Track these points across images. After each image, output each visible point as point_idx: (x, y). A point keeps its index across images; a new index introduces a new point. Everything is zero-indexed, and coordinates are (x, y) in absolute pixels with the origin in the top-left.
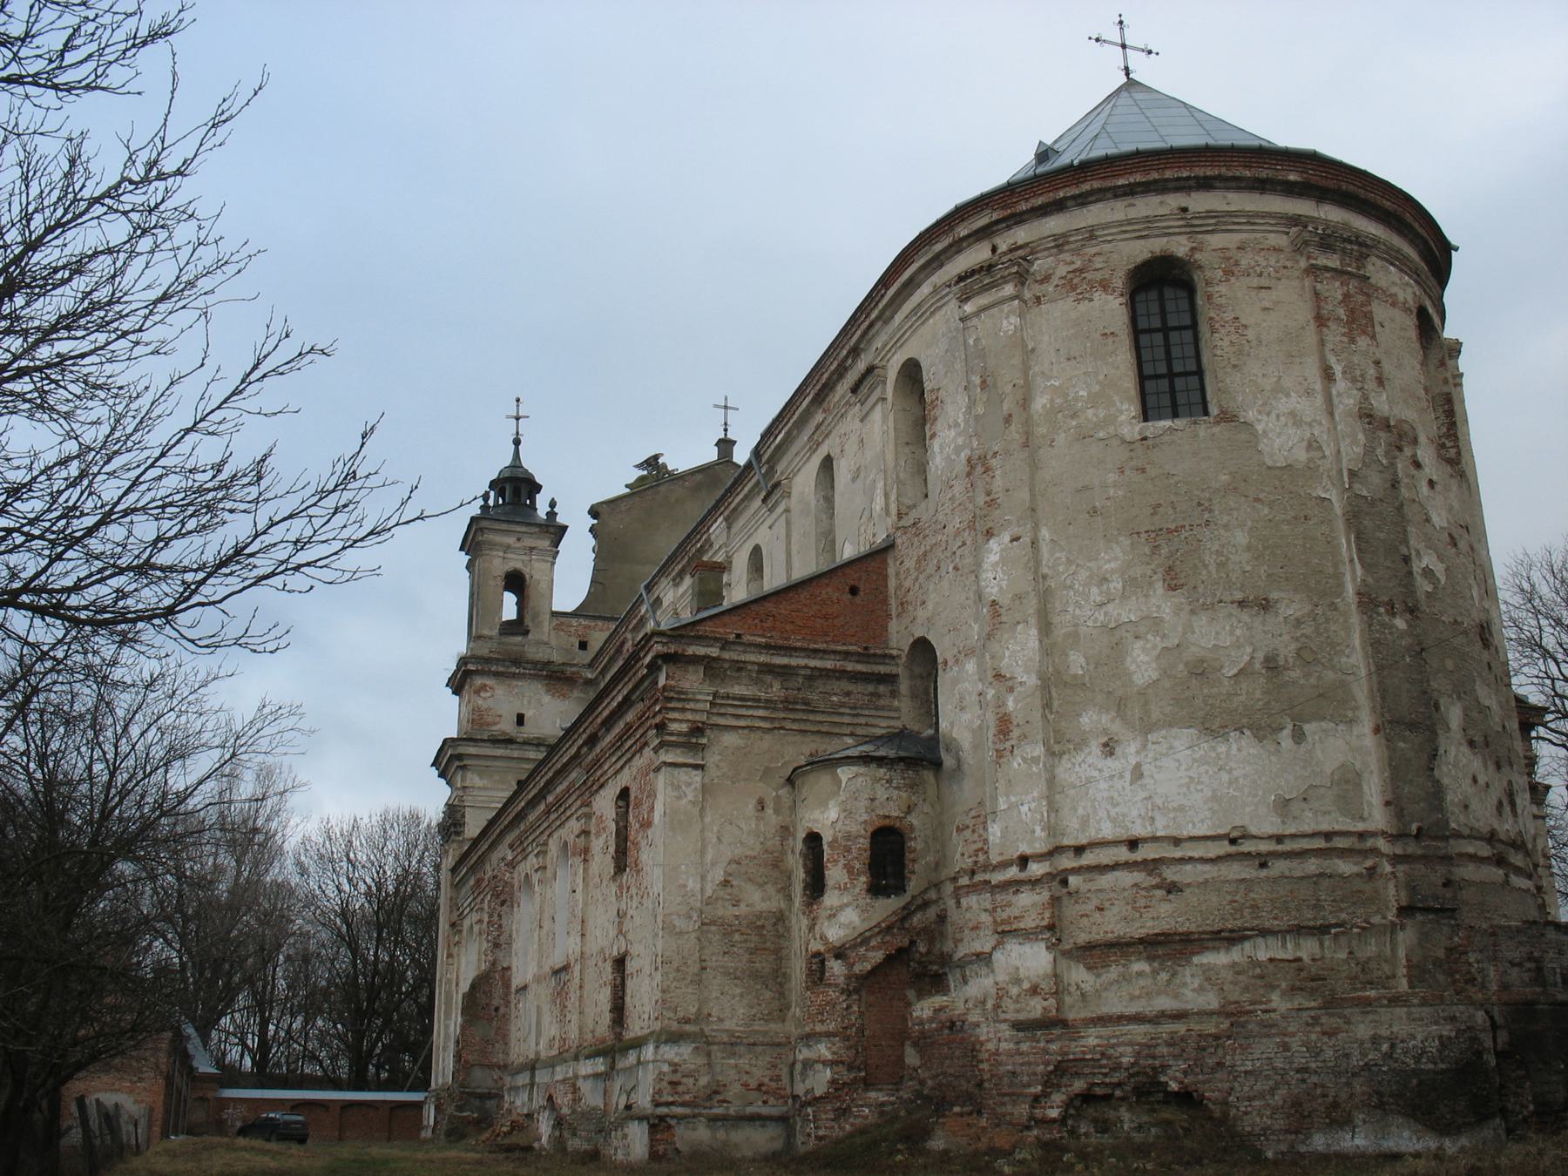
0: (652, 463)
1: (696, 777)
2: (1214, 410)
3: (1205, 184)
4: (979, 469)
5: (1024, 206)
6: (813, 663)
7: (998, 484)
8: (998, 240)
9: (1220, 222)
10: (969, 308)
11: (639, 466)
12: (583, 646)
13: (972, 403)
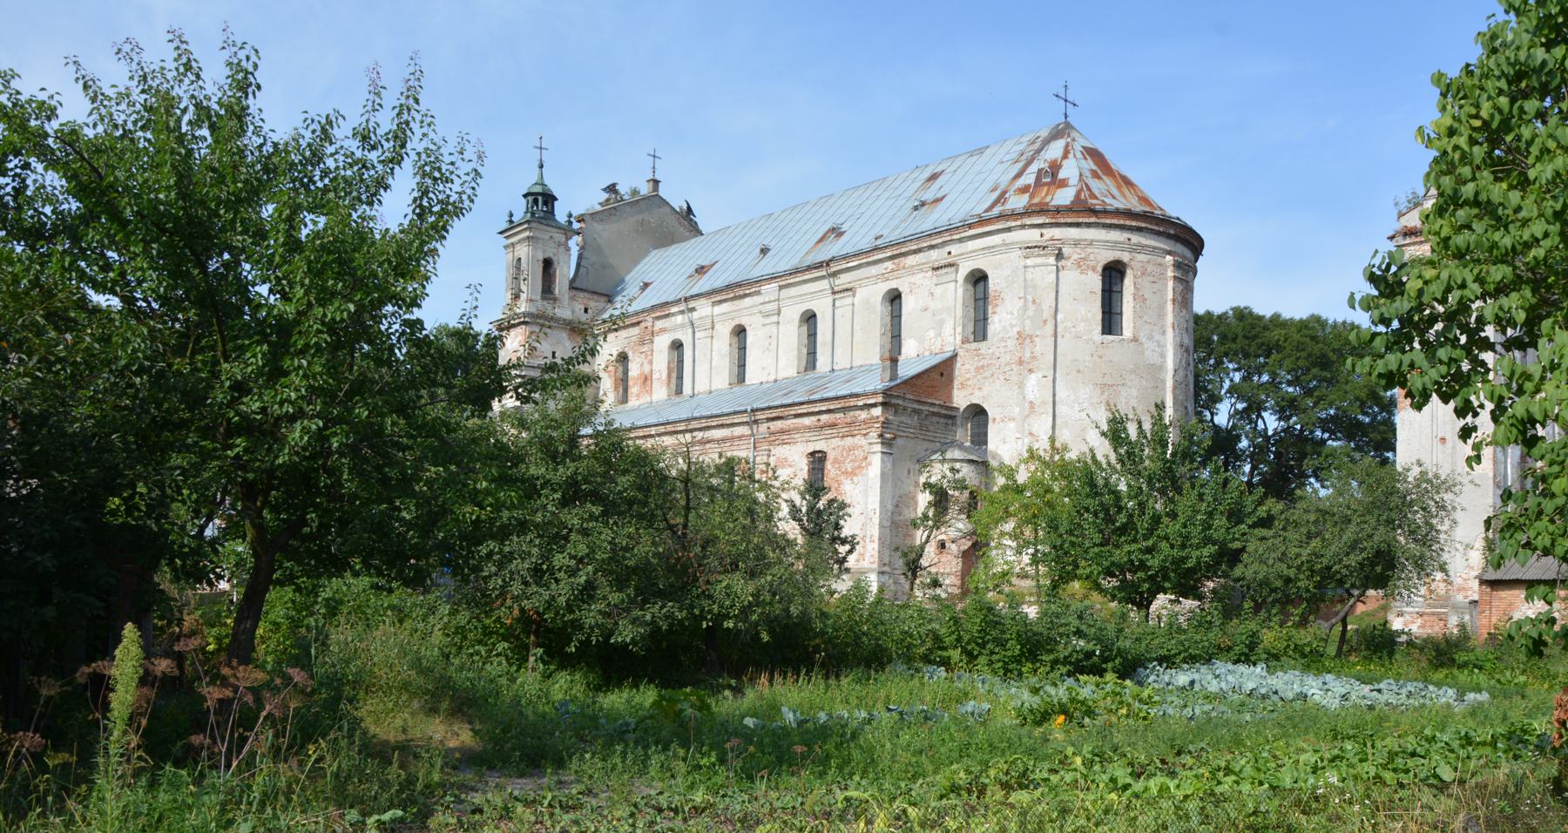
0: (612, 189)
1: (891, 458)
2: (1128, 331)
3: (1139, 230)
4: (1028, 341)
5: (1062, 220)
6: (931, 409)
7: (1038, 350)
8: (1044, 231)
9: (1141, 248)
10: (1029, 262)
11: (604, 190)
12: (586, 311)
13: (1025, 308)
